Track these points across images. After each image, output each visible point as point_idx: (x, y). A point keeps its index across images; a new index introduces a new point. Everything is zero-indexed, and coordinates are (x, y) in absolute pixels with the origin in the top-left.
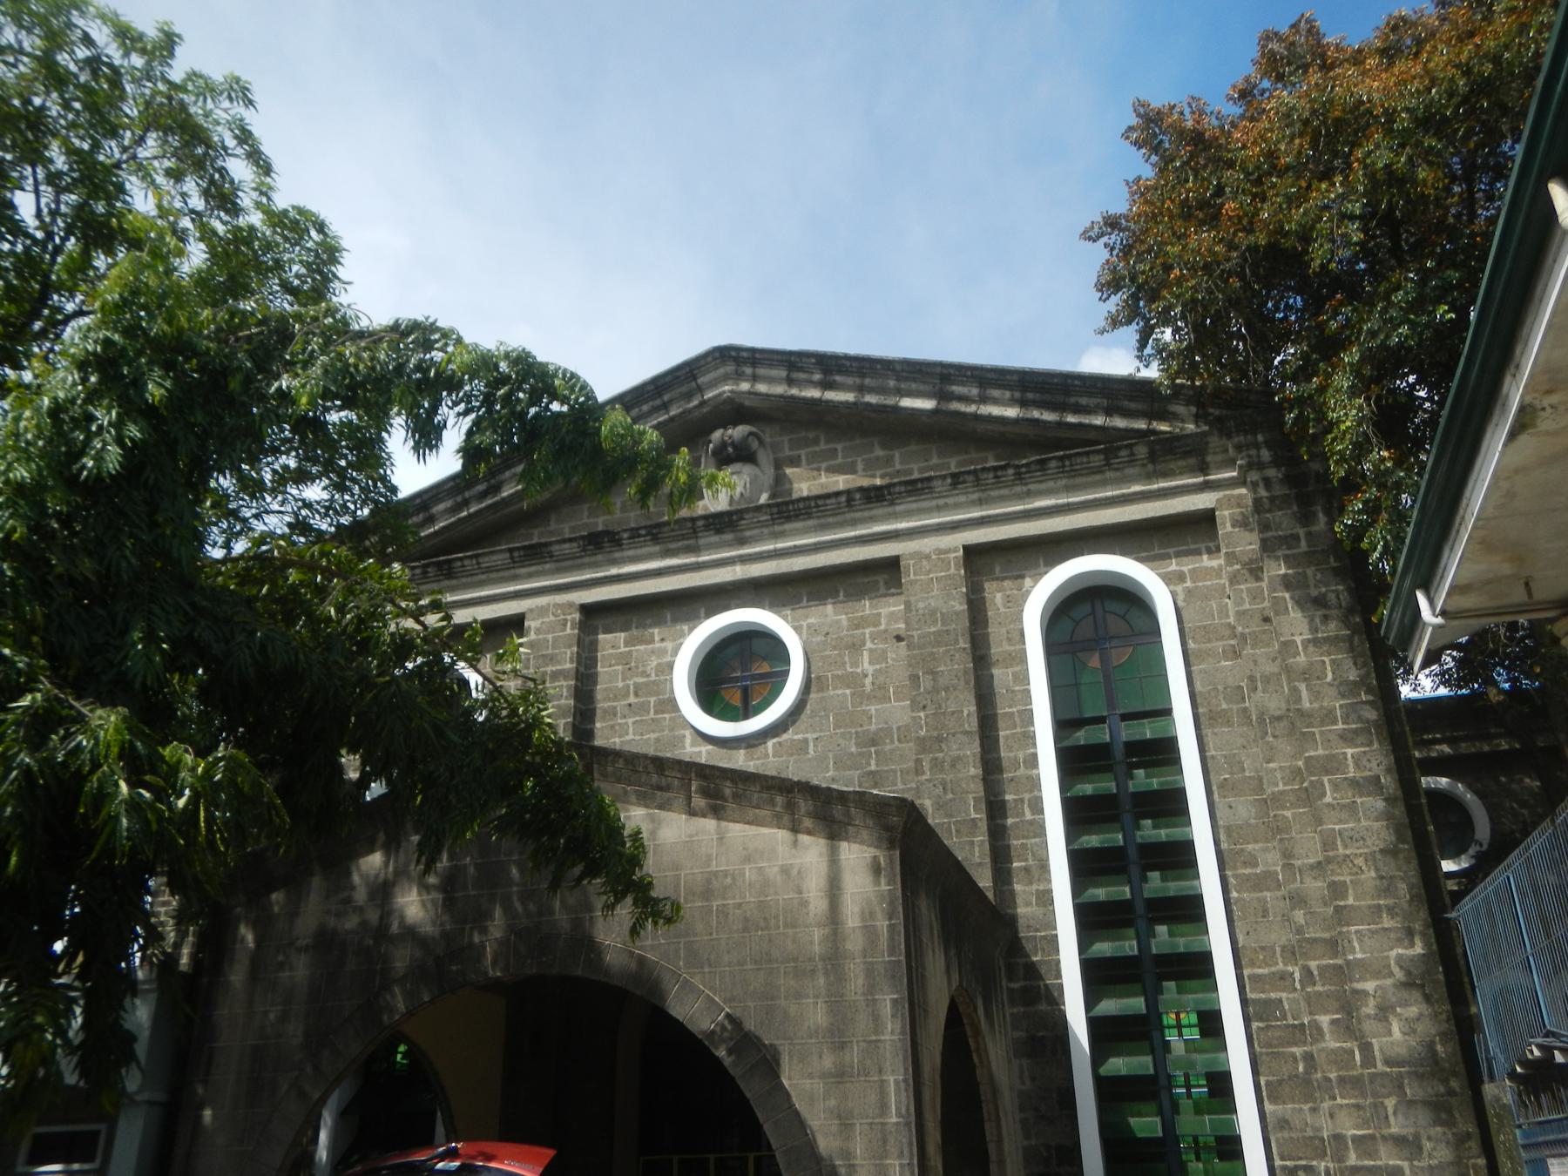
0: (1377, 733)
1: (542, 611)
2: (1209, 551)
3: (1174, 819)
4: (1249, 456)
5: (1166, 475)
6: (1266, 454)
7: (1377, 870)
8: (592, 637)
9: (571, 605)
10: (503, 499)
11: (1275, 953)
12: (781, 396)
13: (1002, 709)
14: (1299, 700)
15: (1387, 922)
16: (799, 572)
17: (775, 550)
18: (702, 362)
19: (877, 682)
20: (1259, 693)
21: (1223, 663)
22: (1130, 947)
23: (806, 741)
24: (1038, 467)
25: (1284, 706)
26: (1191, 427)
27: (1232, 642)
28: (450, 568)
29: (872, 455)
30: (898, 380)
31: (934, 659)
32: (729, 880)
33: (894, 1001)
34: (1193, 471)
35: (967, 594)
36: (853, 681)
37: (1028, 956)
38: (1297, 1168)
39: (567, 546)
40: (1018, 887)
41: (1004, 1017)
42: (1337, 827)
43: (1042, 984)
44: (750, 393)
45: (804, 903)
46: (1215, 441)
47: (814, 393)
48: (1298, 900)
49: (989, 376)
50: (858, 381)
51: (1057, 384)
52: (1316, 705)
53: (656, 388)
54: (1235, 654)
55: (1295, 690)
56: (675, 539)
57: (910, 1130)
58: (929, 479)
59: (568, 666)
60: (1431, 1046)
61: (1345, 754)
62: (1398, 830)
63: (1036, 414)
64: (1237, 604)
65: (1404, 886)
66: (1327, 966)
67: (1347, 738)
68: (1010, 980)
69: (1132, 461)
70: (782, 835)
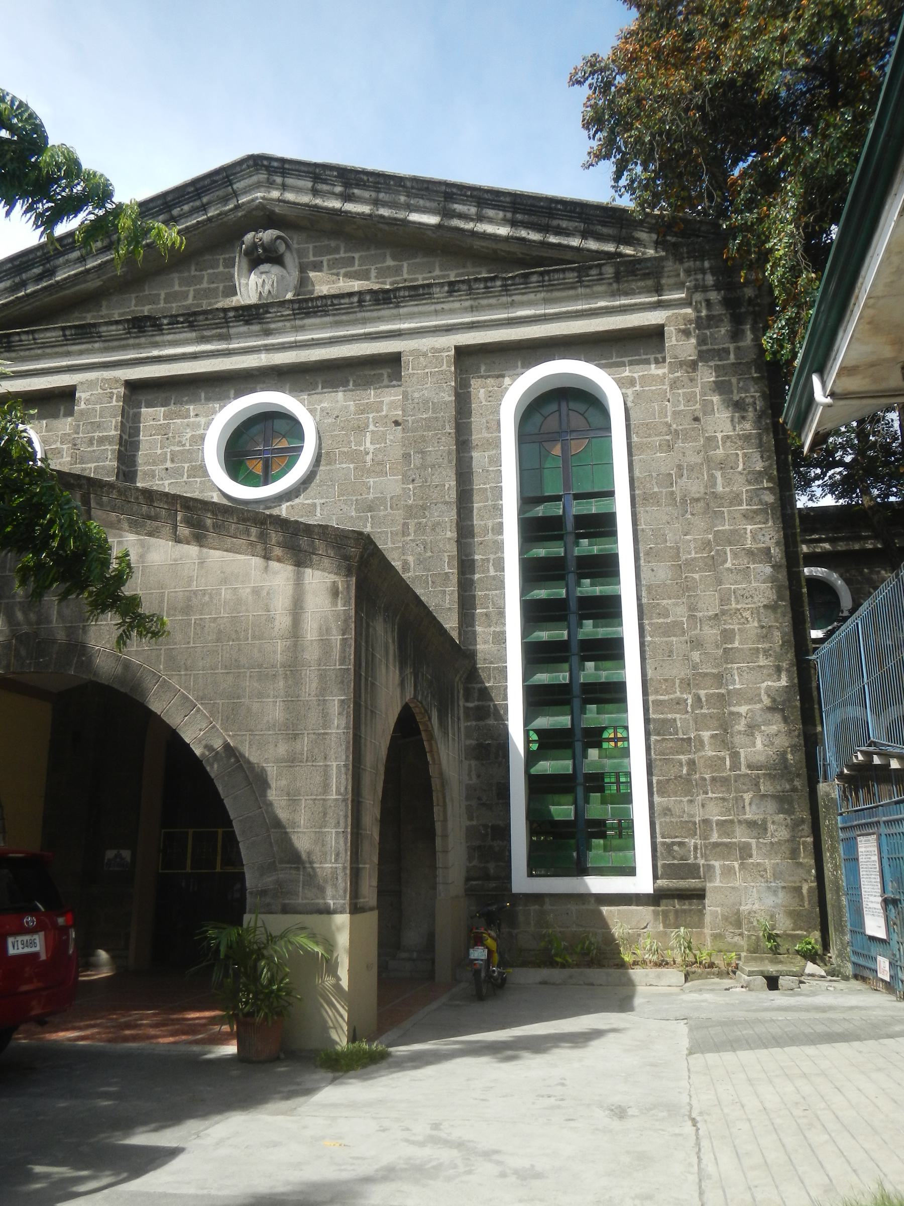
0: (773, 514)
1: (91, 384)
2: (657, 362)
3: (608, 579)
4: (696, 280)
5: (626, 294)
6: (710, 280)
7: (759, 621)
8: (135, 410)
9: (117, 380)
10: (58, 282)
11: (674, 684)
12: (306, 205)
13: (478, 484)
14: (714, 485)
15: (762, 661)
16: (316, 362)
17: (296, 342)
18: (238, 169)
19: (376, 459)
20: (685, 479)
21: (658, 455)
22: (563, 677)
23: (314, 505)
24: (522, 281)
25: (702, 490)
26: (651, 252)
27: (667, 437)
28: (9, 342)
29: (385, 265)
30: (408, 196)
31: (424, 441)
32: (207, 598)
33: (342, 702)
34: (648, 291)
35: (456, 388)
36: (356, 457)
37: (483, 683)
38: (673, 844)
39: (114, 327)
40: (479, 629)
41: (459, 728)
42: (733, 587)
43: (492, 704)
44: (279, 200)
45: (270, 620)
46: (669, 265)
47: (336, 204)
48: (696, 643)
49: (486, 196)
50: (374, 194)
51: (542, 207)
52: (727, 489)
53: (196, 190)
54: (670, 447)
55: (712, 477)
56: (209, 327)
57: (347, 806)
58: (429, 286)
59: (113, 433)
60: (783, 755)
61: (745, 529)
62: (779, 590)
63: (523, 233)
64: (674, 406)
65: (779, 634)
66: (713, 694)
67: (748, 517)
68: (467, 700)
69: (600, 280)
70: (256, 562)
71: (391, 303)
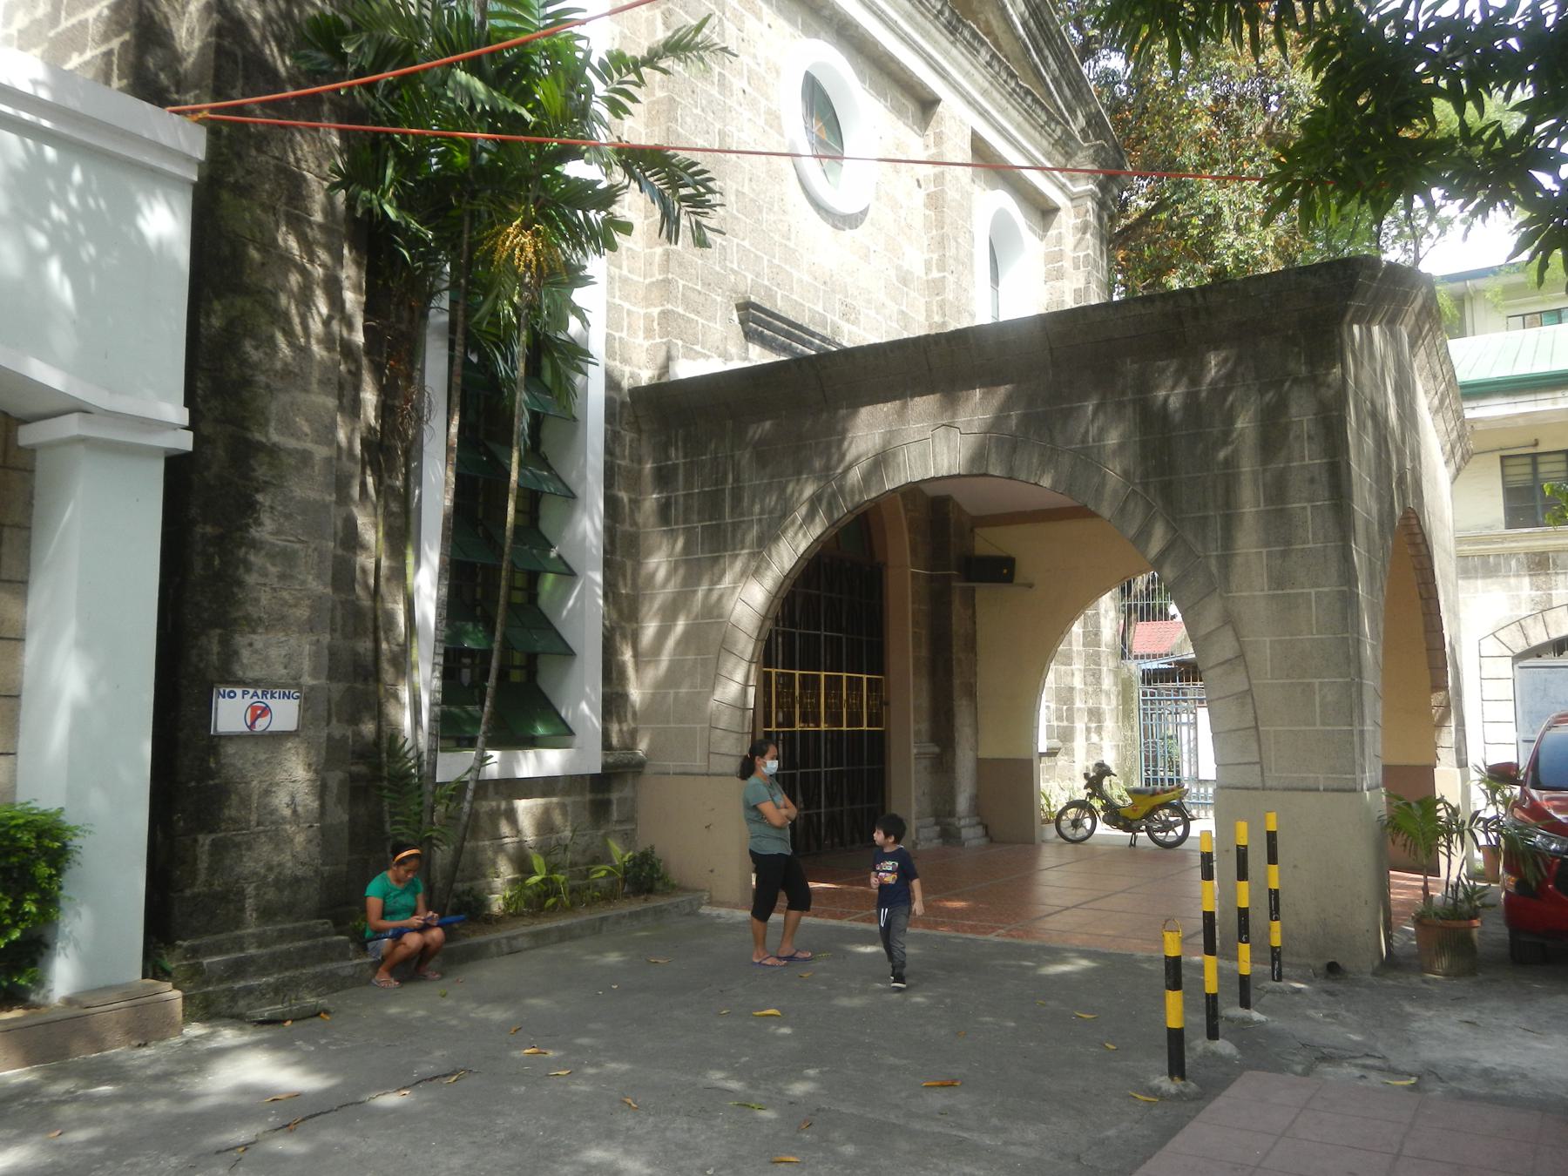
71: (951, 33)
